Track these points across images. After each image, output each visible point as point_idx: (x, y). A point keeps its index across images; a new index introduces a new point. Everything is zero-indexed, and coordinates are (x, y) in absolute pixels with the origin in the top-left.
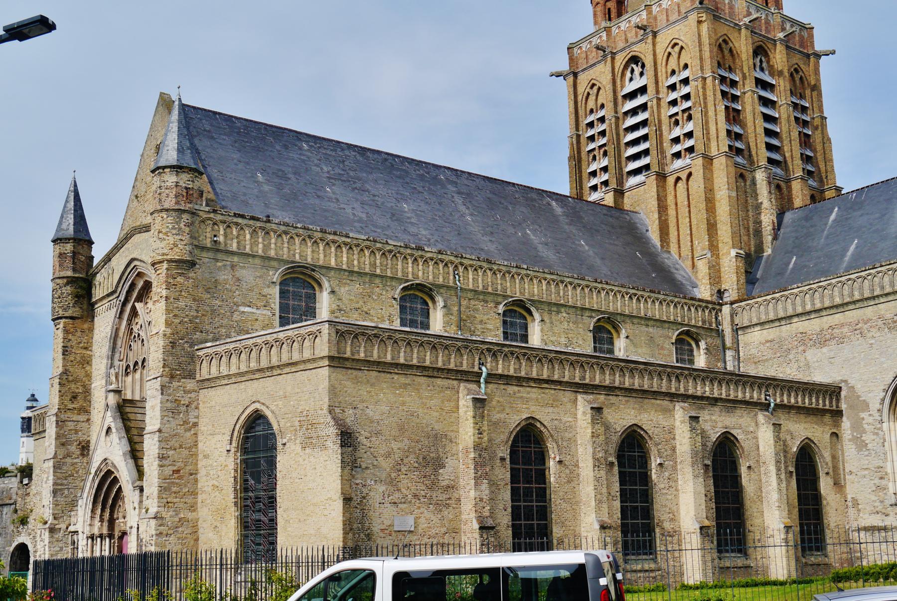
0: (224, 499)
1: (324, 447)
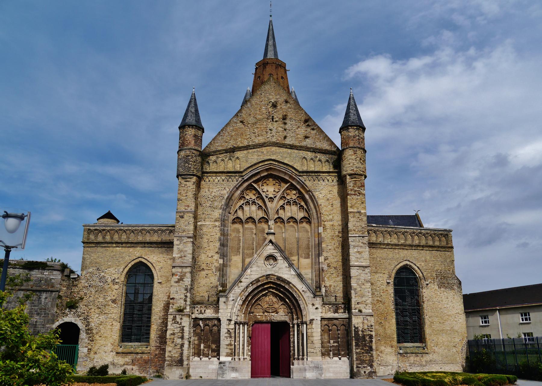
0: (386, 308)
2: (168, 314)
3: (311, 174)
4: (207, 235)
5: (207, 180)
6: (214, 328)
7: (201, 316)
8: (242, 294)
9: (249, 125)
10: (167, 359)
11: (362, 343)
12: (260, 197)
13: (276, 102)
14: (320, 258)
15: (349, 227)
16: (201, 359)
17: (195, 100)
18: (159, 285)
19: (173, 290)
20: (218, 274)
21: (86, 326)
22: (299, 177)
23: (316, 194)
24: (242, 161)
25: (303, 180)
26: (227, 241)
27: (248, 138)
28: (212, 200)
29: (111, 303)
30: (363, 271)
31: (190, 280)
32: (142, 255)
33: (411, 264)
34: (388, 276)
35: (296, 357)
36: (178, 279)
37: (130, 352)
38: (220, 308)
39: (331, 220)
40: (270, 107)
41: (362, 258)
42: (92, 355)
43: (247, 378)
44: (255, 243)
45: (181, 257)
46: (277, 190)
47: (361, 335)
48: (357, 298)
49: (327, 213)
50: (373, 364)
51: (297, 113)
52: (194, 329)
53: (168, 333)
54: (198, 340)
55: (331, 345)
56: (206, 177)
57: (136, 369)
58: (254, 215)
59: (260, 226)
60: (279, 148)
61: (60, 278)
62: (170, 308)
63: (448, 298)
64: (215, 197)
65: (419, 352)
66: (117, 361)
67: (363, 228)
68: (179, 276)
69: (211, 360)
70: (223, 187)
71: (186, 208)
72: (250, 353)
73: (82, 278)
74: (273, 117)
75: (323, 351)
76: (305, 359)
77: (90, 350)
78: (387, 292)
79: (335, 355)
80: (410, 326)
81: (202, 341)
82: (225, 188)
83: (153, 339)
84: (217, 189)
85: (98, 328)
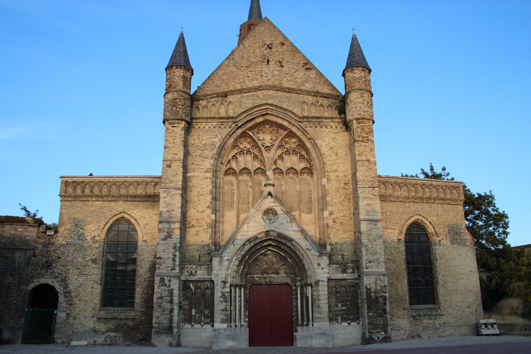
0: (397, 267)
1: (465, 245)
2: (155, 275)
3: (312, 120)
4: (197, 188)
5: (197, 127)
6: (207, 291)
7: (192, 278)
8: (238, 253)
9: (242, 69)
10: (154, 325)
11: (375, 306)
12: (255, 145)
13: (271, 44)
14: (324, 212)
15: (357, 176)
16: (192, 326)
17: (184, 40)
18: (145, 243)
19: (160, 248)
20: (210, 231)
21: (64, 289)
22: (299, 123)
23: (318, 142)
24: (236, 106)
25: (304, 127)
26: (220, 195)
27: (241, 83)
28: (202, 149)
29: (91, 263)
30: (375, 225)
31: (179, 237)
32: (124, 210)
33: (422, 218)
34: (399, 232)
35: (300, 322)
36: (166, 236)
37: (113, 317)
38: (213, 269)
39: (336, 171)
40: (264, 49)
41: (373, 211)
42: (71, 320)
43: (245, 347)
44: (250, 197)
45: (168, 212)
46: (274, 138)
47: (373, 297)
48: (368, 256)
49: (331, 163)
50: (388, 328)
51: (295, 56)
52: (184, 292)
53: (155, 296)
54: (188, 304)
55: (339, 309)
56: (195, 124)
57: (120, 337)
58: (249, 166)
59: (256, 178)
60: (276, 92)
61: (35, 234)
62: (157, 268)
63: (461, 255)
64: (205, 145)
65: (433, 314)
66: (99, 328)
67: (373, 178)
68: (166, 233)
69: (204, 327)
70: (215, 134)
71: (174, 156)
72: (247, 319)
73: (59, 235)
74: (268, 59)
75: (330, 315)
76: (311, 325)
77: (68, 315)
78: (398, 249)
79: (343, 320)
80: (422, 286)
81: (193, 306)
82: (216, 136)
83: (138, 303)
84: (208, 137)
85: (77, 291)
